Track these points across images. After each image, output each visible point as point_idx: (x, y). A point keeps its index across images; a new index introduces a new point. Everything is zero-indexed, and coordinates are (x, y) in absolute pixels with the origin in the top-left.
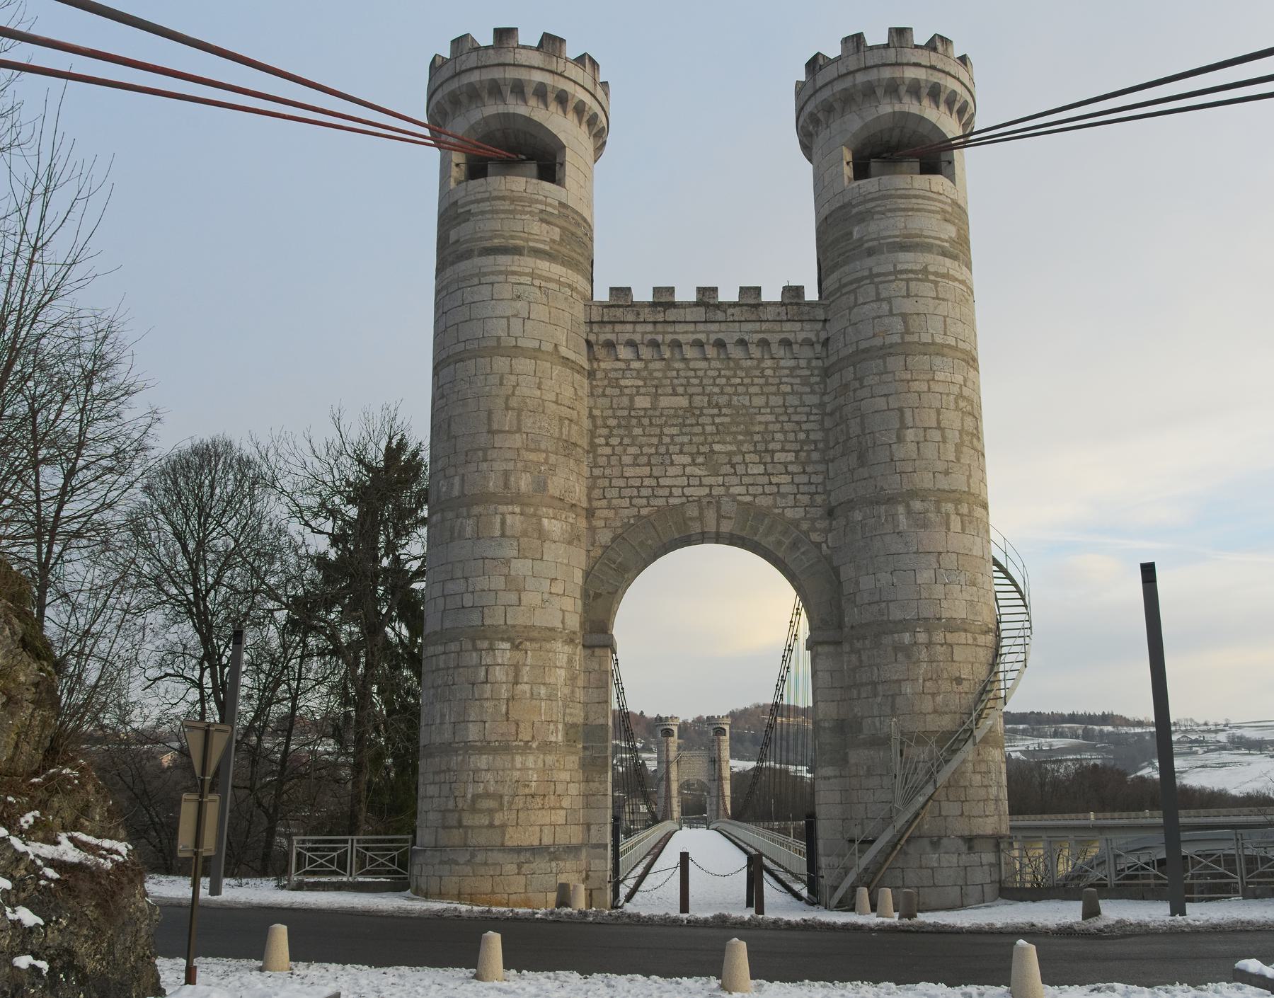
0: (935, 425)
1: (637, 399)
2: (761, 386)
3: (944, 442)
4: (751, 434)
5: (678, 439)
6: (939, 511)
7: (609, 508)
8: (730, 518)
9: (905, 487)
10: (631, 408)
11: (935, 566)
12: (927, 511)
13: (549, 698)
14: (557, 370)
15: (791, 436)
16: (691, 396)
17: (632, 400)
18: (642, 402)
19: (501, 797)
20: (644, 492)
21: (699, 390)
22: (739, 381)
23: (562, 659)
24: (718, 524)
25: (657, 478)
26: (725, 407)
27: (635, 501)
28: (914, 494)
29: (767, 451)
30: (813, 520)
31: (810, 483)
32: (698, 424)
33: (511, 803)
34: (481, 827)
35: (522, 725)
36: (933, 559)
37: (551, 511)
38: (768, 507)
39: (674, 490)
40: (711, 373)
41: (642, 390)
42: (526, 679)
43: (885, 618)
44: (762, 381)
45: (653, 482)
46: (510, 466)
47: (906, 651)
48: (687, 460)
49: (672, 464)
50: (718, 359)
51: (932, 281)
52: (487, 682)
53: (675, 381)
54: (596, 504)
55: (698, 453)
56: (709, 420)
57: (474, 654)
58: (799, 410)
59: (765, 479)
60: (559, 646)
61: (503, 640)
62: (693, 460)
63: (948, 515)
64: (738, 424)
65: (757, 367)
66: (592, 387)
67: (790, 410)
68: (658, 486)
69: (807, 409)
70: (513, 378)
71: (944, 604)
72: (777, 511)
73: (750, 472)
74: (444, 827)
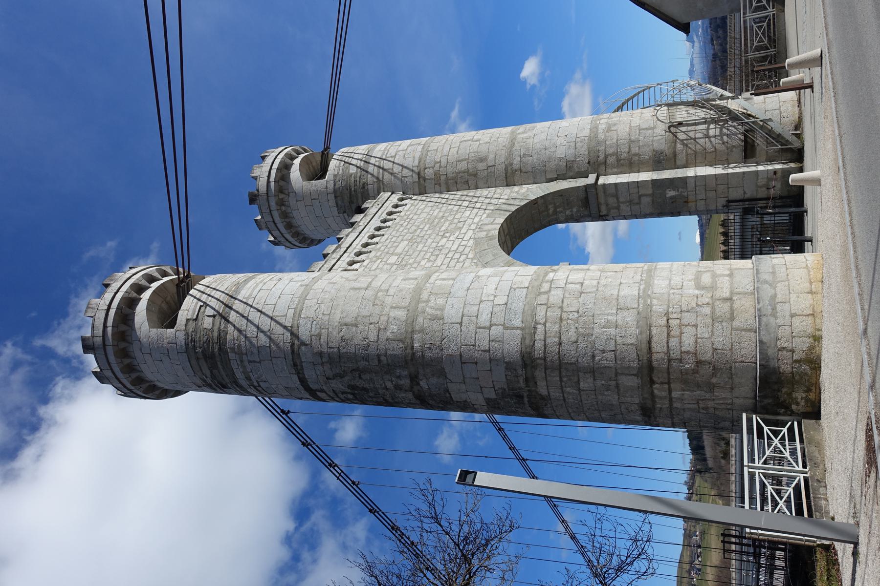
34: (732, 283)
52: (582, 284)
74: (732, 319)
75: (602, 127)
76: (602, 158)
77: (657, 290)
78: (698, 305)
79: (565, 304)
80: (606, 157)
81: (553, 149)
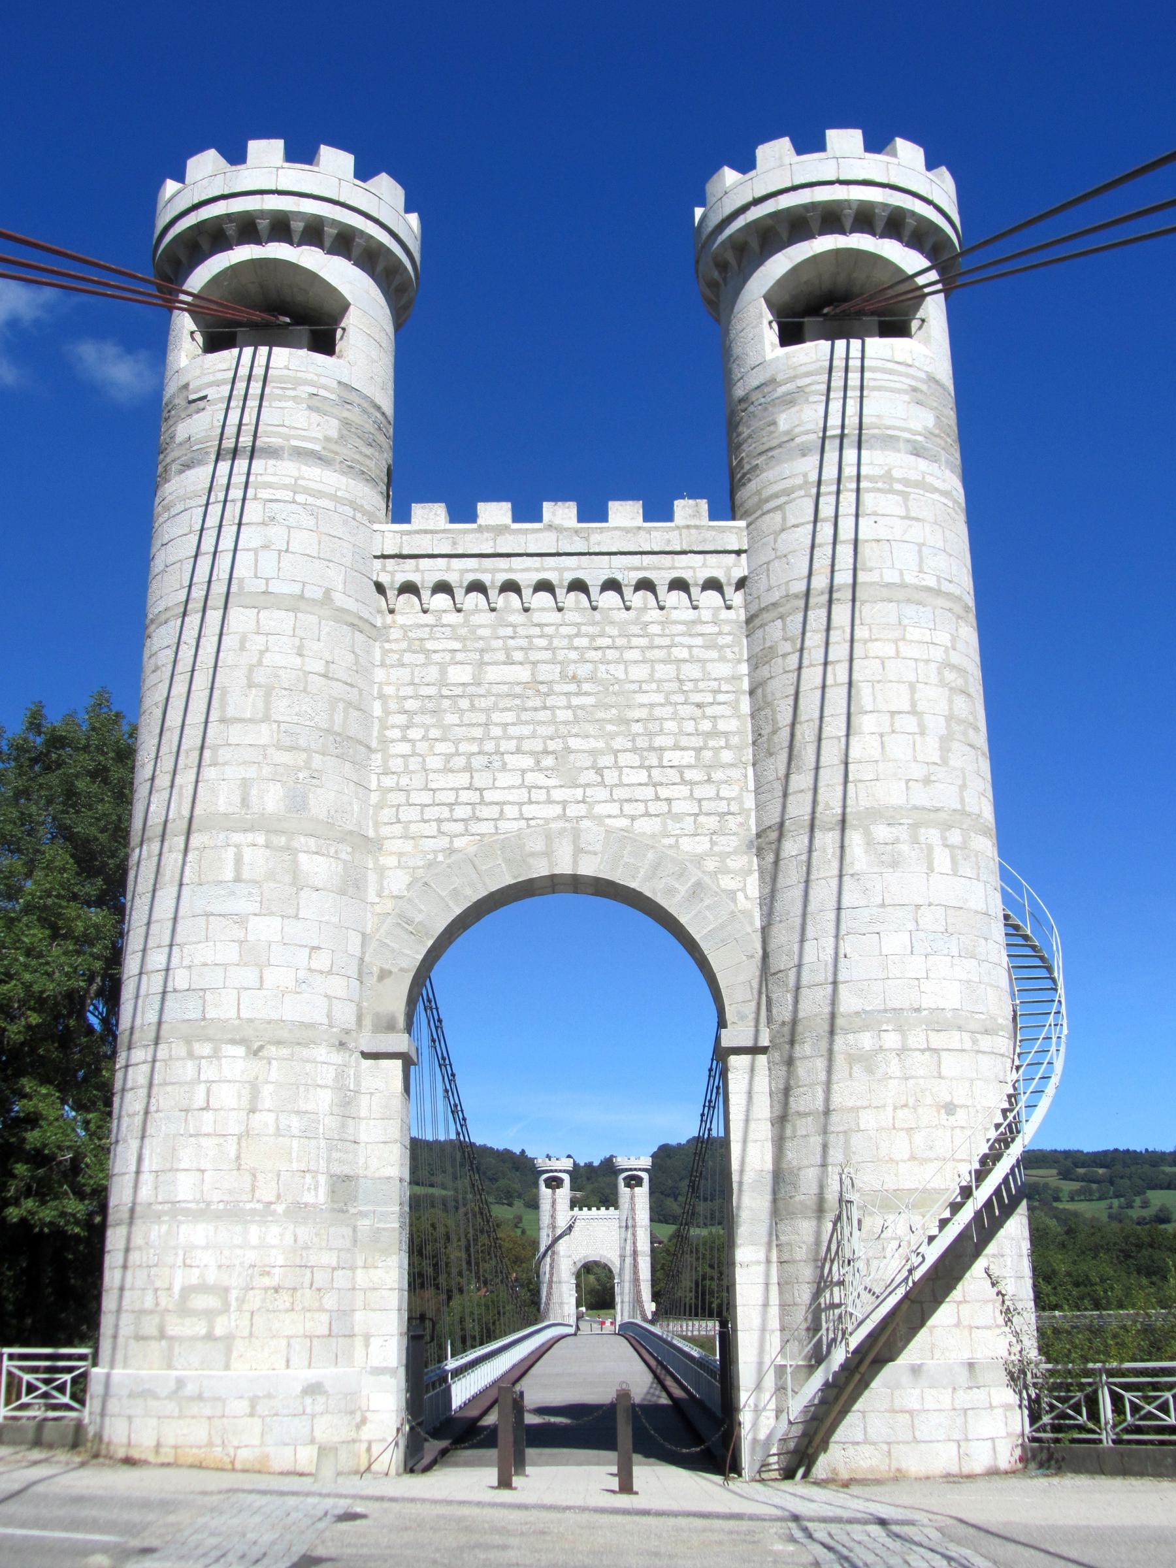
0: (907, 708)
1: (451, 670)
2: (643, 649)
3: (922, 733)
4: (627, 722)
5: (512, 730)
6: (915, 841)
7: (406, 837)
8: (595, 854)
10: (442, 683)
11: (911, 926)
13: (306, 1135)
14: (328, 627)
15: (689, 726)
16: (534, 663)
17: (443, 672)
18: (460, 674)
19: (227, 1290)
20: (461, 812)
21: (547, 655)
22: (607, 641)
23: (327, 1075)
24: (575, 863)
25: (480, 790)
26: (587, 680)
27: (447, 827)
29: (652, 748)
30: (724, 856)
31: (718, 797)
32: (545, 708)
33: (241, 1301)
34: (194, 1338)
35: (260, 1176)
37: (312, 842)
38: (653, 836)
39: (506, 808)
40: (564, 630)
41: (460, 656)
42: (267, 1106)
44: (643, 642)
45: (474, 797)
46: (251, 772)
48: (527, 762)
49: (504, 767)
50: (578, 609)
51: (898, 493)
52: (207, 1108)
53: (511, 642)
54: (385, 831)
55: (546, 752)
56: (562, 701)
57: (190, 1064)
58: (701, 685)
59: (649, 792)
60: (321, 1053)
61: (233, 1042)
62: (538, 762)
63: (930, 848)
64: (608, 707)
65: (636, 622)
66: (385, 652)
67: (688, 686)
68: (482, 802)
69: (715, 685)
70: (261, 639)
72: (666, 841)
73: (625, 780)
77: (183, 1229)
78: (156, 1290)
79: (169, 1088)
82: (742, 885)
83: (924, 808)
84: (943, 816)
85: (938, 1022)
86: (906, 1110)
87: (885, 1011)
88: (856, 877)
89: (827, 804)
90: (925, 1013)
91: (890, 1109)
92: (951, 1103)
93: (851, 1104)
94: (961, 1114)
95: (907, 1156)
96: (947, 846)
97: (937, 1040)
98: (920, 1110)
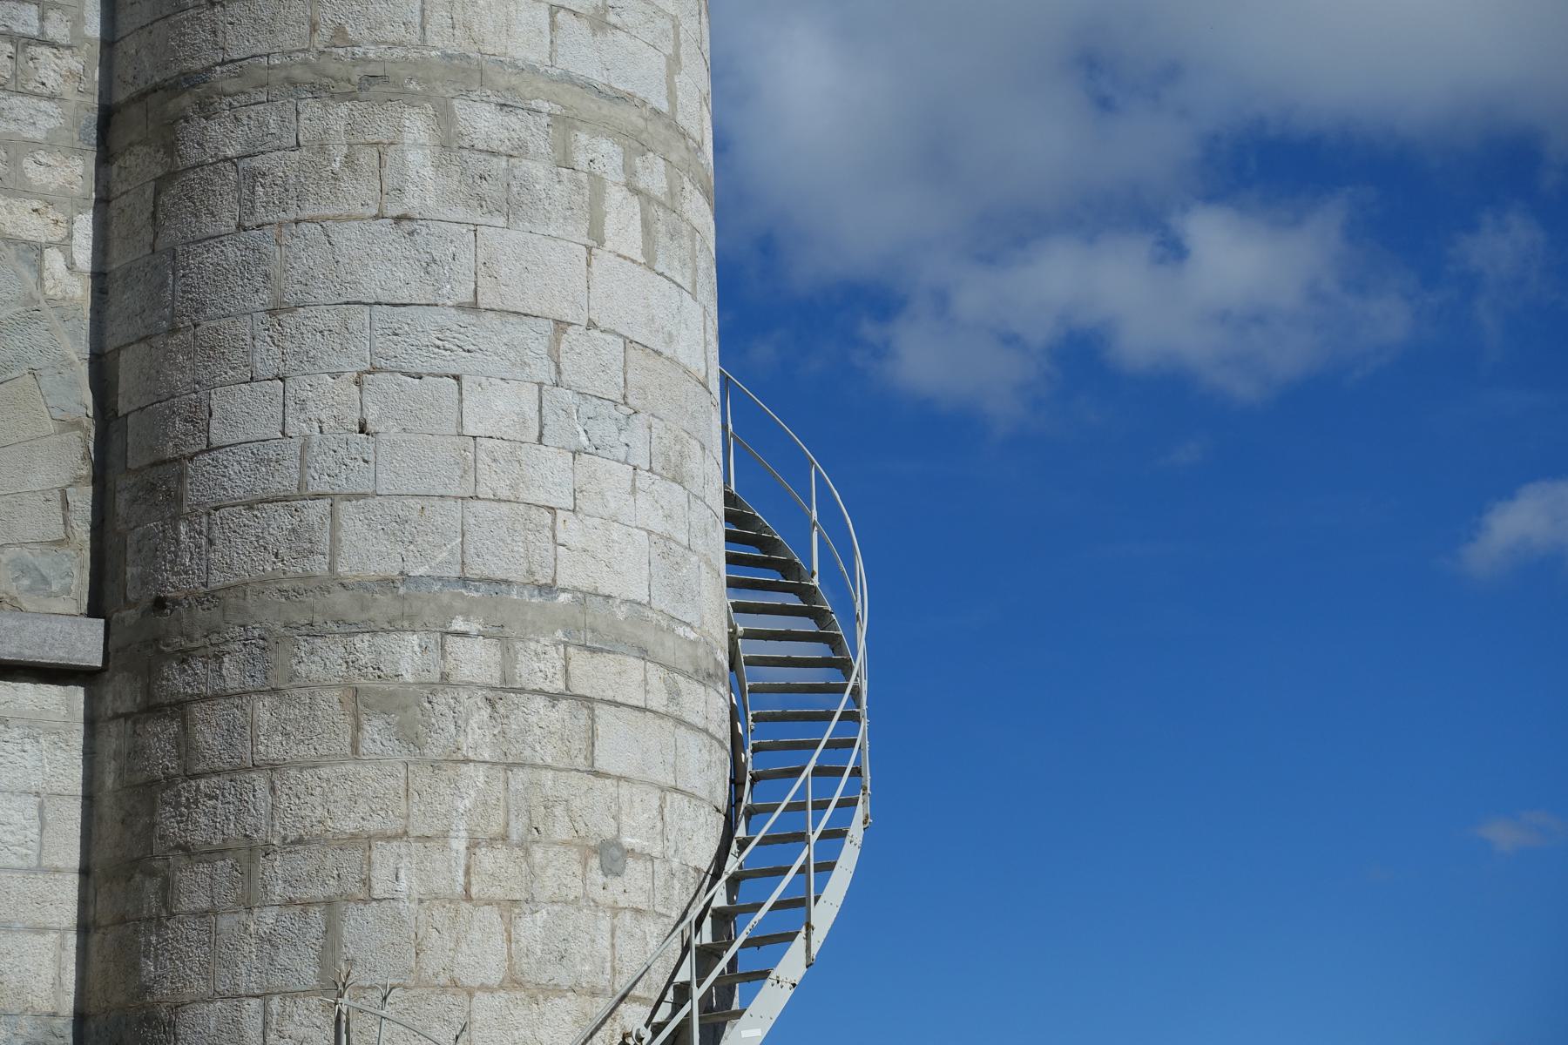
6: (564, 161)
9: (441, 41)
11: (544, 372)
12: (519, 151)
28: (469, 73)
36: (535, 340)
43: (319, 565)
47: (403, 710)
71: (570, 530)
75: (408, 656)
76: (177, 681)
80: (179, 708)
81: (266, 359)
82: (60, 232)
83: (587, 86)
84: (629, 117)
85: (595, 627)
86: (501, 853)
87: (464, 581)
88: (406, 225)
89: (340, 30)
90: (563, 598)
91: (459, 844)
92: (615, 843)
93: (349, 826)
94: (634, 868)
95: (495, 978)
96: (636, 191)
97: (592, 674)
98: (538, 854)
